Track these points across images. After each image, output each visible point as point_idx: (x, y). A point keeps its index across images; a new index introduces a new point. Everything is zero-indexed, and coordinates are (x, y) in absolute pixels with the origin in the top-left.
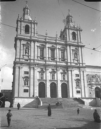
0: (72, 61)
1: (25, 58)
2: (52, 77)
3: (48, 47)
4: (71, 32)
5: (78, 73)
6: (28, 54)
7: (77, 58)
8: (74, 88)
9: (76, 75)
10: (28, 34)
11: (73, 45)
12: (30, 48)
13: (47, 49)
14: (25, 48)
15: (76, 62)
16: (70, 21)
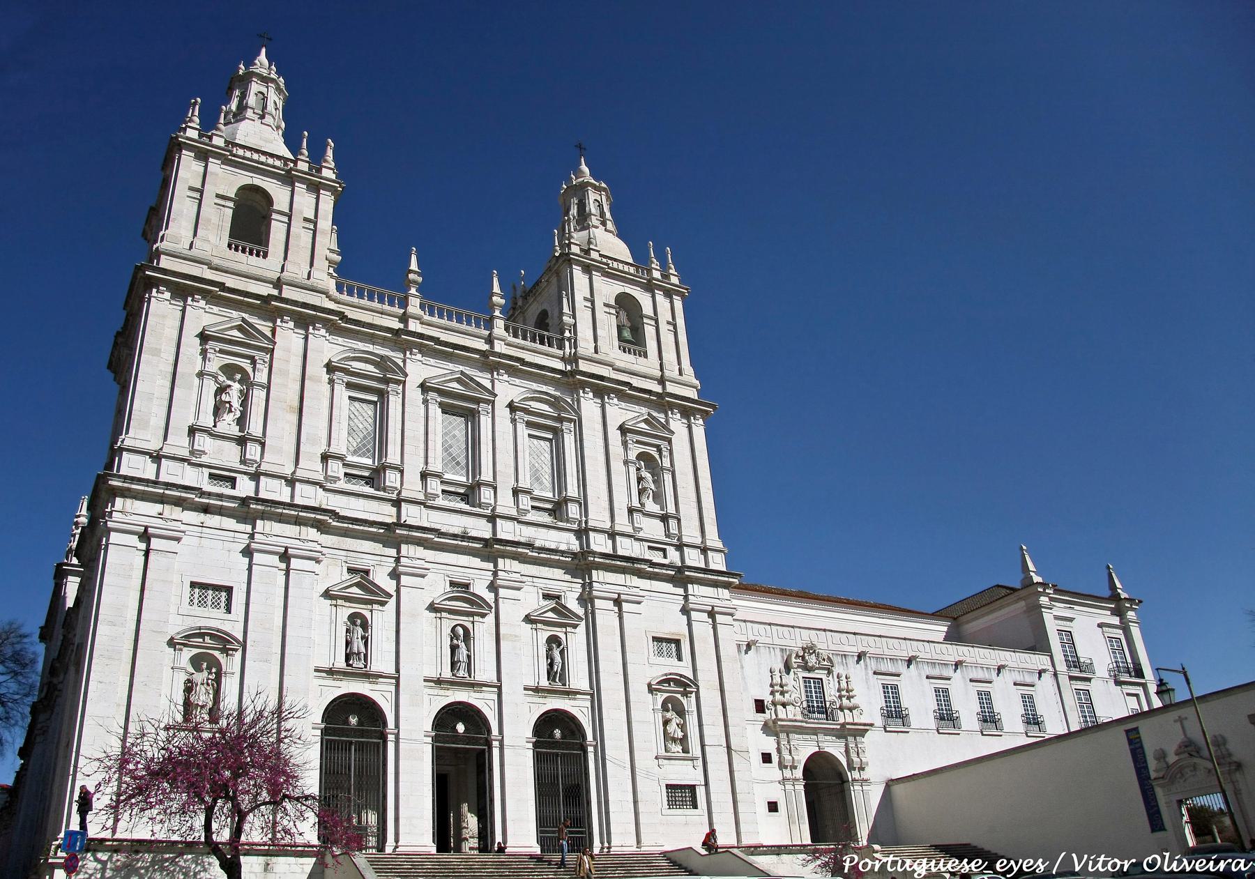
0: (622, 523)
1: (204, 459)
2: (454, 649)
3: (424, 387)
5: (675, 625)
6: (242, 421)
7: (658, 497)
8: (645, 760)
9: (655, 639)
10: (253, 260)
11: (626, 393)
12: (262, 377)
13: (414, 395)
14: (215, 363)
15: (654, 529)
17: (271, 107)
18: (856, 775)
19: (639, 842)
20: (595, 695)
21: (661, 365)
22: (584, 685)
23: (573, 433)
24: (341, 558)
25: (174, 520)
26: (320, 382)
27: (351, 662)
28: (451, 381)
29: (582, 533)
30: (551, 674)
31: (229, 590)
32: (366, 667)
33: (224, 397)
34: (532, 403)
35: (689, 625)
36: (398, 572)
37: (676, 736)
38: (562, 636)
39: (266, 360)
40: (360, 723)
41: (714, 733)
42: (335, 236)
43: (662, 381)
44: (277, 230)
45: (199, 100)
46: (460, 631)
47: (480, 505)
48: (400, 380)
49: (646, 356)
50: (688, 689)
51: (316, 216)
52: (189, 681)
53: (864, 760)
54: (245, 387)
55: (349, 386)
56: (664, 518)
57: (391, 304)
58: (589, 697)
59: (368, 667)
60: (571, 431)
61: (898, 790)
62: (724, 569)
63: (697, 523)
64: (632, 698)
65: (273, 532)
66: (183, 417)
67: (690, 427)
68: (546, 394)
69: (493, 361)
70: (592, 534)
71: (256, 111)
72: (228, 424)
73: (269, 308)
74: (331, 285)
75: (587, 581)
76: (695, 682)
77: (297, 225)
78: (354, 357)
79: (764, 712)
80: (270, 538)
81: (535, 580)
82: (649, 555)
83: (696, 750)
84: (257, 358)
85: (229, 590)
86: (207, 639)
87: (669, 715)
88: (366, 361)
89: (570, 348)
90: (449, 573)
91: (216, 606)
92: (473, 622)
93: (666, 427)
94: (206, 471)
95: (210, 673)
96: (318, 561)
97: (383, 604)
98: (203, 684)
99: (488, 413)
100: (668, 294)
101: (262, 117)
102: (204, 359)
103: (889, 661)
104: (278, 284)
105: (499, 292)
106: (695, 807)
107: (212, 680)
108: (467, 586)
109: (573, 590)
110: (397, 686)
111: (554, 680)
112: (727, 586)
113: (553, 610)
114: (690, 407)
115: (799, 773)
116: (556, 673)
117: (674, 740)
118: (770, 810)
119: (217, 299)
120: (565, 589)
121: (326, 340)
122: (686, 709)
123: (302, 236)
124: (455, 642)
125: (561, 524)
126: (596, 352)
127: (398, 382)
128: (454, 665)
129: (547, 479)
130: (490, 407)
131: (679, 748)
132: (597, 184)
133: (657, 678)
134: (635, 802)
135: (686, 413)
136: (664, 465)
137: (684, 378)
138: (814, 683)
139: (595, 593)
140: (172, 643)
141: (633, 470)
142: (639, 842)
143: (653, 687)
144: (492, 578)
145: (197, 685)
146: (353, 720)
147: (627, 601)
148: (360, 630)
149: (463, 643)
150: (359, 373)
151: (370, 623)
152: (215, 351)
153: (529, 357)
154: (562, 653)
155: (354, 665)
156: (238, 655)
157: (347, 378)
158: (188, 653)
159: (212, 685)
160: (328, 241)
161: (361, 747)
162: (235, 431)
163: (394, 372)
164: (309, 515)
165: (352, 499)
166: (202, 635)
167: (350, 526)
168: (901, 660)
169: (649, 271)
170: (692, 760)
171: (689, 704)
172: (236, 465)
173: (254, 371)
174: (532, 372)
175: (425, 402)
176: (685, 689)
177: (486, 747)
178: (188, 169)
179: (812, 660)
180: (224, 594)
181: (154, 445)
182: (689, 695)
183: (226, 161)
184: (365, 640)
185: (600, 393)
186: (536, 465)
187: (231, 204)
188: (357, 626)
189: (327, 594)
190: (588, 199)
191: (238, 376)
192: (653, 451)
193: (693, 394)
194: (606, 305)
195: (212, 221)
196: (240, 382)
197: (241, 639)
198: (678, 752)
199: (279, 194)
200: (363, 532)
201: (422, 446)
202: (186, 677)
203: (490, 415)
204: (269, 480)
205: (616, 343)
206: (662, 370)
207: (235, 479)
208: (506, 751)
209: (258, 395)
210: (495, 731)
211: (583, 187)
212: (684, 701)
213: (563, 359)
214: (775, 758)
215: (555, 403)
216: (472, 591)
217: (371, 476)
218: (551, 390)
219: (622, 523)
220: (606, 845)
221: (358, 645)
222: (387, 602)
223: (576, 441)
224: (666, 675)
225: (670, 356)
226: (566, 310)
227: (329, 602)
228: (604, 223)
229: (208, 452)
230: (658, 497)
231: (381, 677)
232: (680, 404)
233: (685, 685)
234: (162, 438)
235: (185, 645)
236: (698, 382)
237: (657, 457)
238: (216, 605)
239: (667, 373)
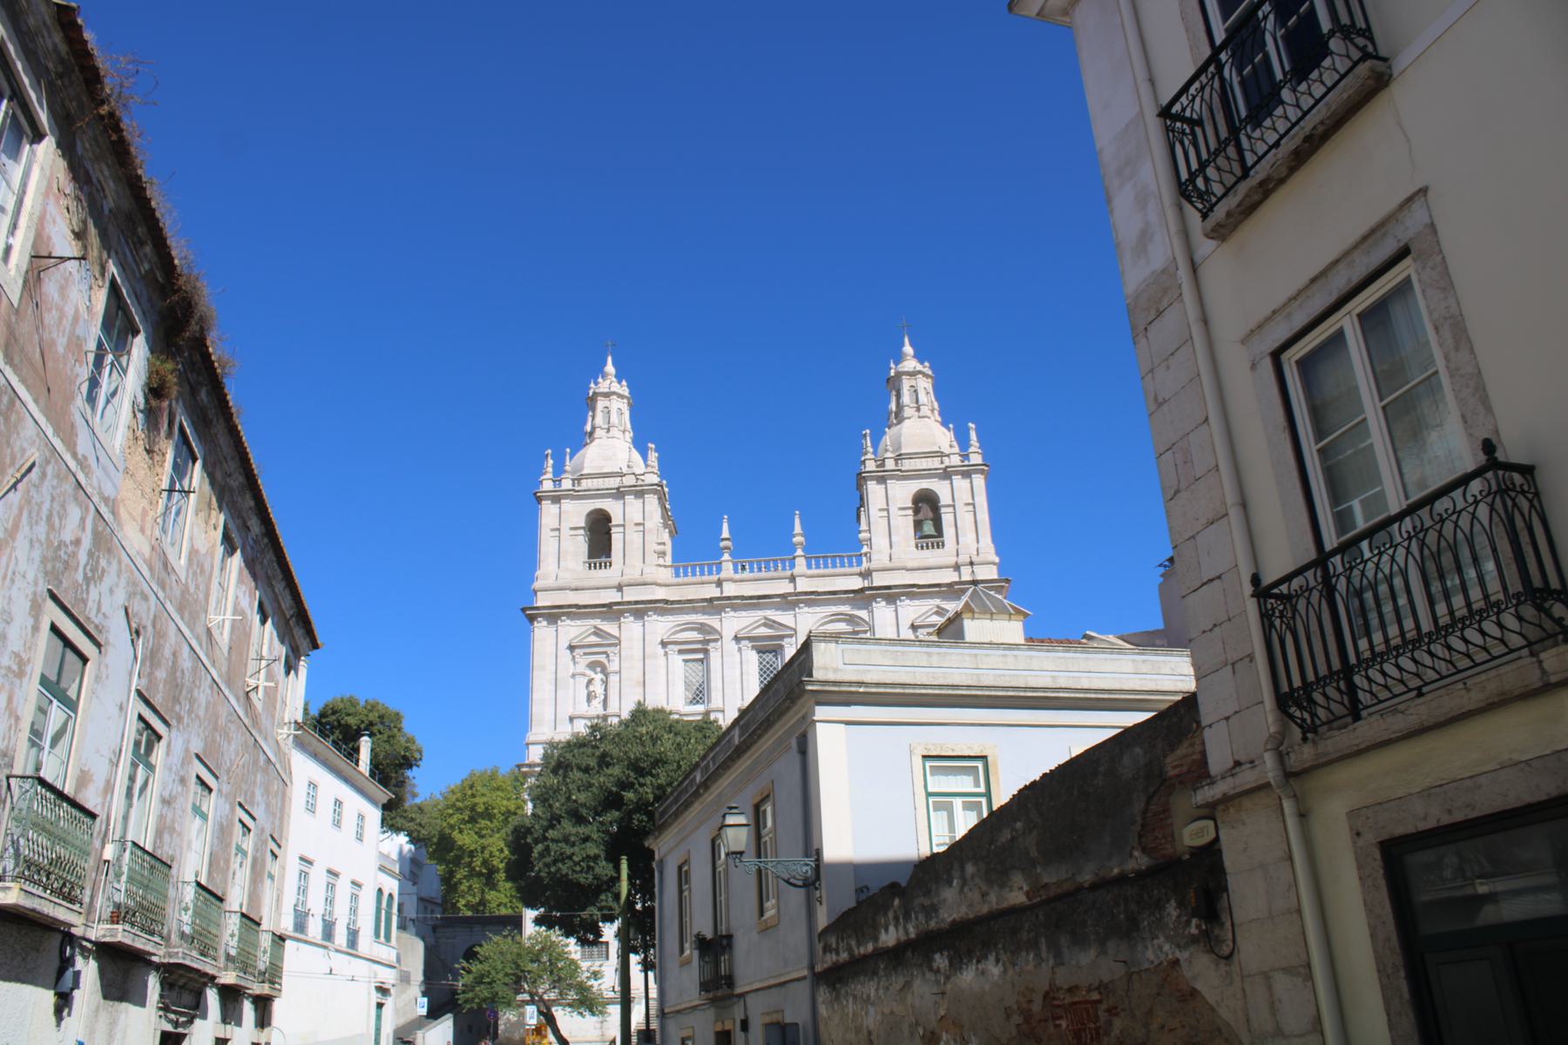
3: (737, 639)
4: (903, 492)
17: (614, 418)
33: (591, 689)
55: (681, 652)
73: (611, 611)
77: (630, 529)
101: (608, 431)
127: (716, 640)
178: (548, 511)
187: (582, 532)
201: (738, 686)
209: (613, 679)
215: (851, 619)
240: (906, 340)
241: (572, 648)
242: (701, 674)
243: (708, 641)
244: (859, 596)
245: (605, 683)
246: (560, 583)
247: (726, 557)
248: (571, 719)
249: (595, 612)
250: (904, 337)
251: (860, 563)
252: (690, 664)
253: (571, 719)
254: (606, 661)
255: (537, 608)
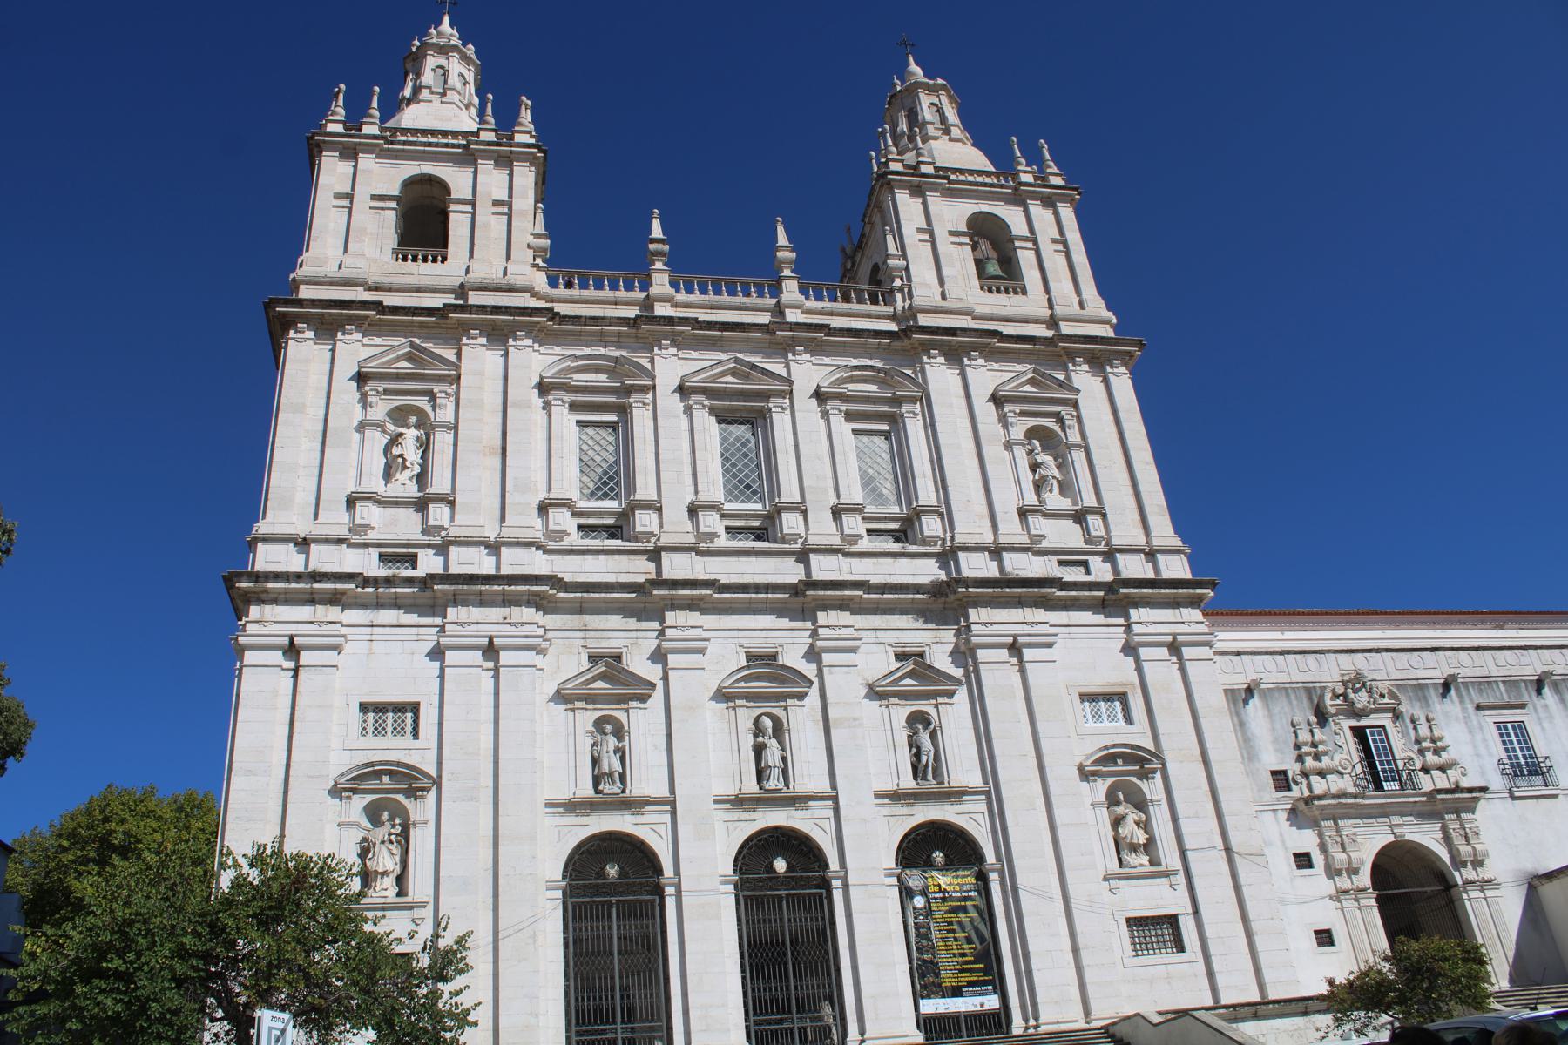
0: (1011, 531)
1: (372, 536)
2: (759, 750)
3: (683, 390)
4: (952, 213)
5: (1116, 672)
6: (422, 479)
8: (1085, 885)
10: (429, 268)
14: (380, 408)
15: (1066, 535)
16: (931, 130)
17: (454, 80)
18: (1469, 873)
19: (1087, 1012)
20: (992, 794)
21: (1050, 300)
22: (974, 779)
23: (920, 417)
24: (578, 641)
25: (331, 622)
26: (530, 407)
27: (601, 788)
28: (723, 374)
29: (948, 556)
30: (917, 770)
31: (415, 708)
32: (623, 791)
33: (396, 451)
34: (851, 386)
35: (1139, 669)
36: (663, 652)
37: (1135, 841)
38: (931, 710)
39: (449, 391)
40: (622, 874)
41: (1200, 829)
42: (540, 217)
43: (1053, 322)
44: (458, 225)
45: (343, 86)
46: (768, 723)
47: (783, 538)
48: (645, 386)
49: (1024, 292)
50: (1146, 766)
51: (510, 196)
52: (365, 839)
53: (1478, 847)
54: (422, 432)
55: (574, 407)
56: (1079, 517)
57: (629, 288)
58: (983, 797)
59: (628, 791)
60: (915, 414)
61: (1548, 891)
62: (1188, 576)
63: (1136, 516)
64: (1053, 790)
65: (470, 620)
66: (341, 483)
67: (1106, 381)
68: (871, 368)
69: (783, 337)
70: (962, 556)
71: (434, 90)
72: (404, 486)
74: (540, 280)
75: (963, 624)
76: (1158, 755)
77: (485, 212)
78: (578, 367)
79: (1289, 789)
80: (467, 628)
81: (880, 634)
82: (1055, 571)
83: (1171, 859)
84: (436, 391)
85: (415, 708)
86: (386, 779)
87: (1120, 810)
88: (597, 370)
89: (904, 301)
90: (743, 642)
91: (399, 732)
92: (786, 708)
93: (1066, 385)
94: (375, 552)
95: (393, 826)
96: (541, 651)
97: (643, 699)
98: (383, 842)
99: (783, 409)
100: (1049, 202)
101: (444, 94)
102: (364, 408)
103: (1501, 685)
104: (462, 291)
105: (787, 244)
106: (1182, 949)
107: (397, 835)
108: (774, 656)
109: (943, 640)
110: (674, 813)
111: (924, 778)
112: (1194, 602)
113: (910, 674)
114: (1101, 350)
115: (1365, 879)
116: (926, 766)
117: (1134, 848)
118: (1320, 944)
119: (377, 325)
120: (928, 641)
121: (534, 351)
122: (1149, 797)
123: (492, 225)
124: (761, 739)
125: (913, 548)
126: (944, 298)
127: (643, 390)
128: (761, 775)
129: (887, 488)
130: (787, 401)
131: (1145, 859)
132: (931, 82)
133: (1092, 754)
134: (1076, 951)
135: (1098, 363)
136: (1070, 439)
137: (1087, 313)
138: (1372, 734)
139: (974, 640)
140: (336, 792)
141: (1021, 454)
142: (1087, 1012)
143: (1087, 768)
144: (810, 640)
145: (374, 844)
146: (612, 871)
147: (1030, 645)
148: (612, 742)
149: (774, 742)
150: (586, 387)
151: (626, 728)
152: (378, 392)
153: (836, 322)
154: (933, 735)
155: (605, 791)
156: (432, 795)
157: (568, 398)
158: (360, 802)
159: (399, 842)
160: (529, 225)
161: (627, 911)
162: (412, 491)
163: (634, 376)
164: (519, 588)
165: (589, 559)
166: (378, 774)
167: (585, 595)
168: (1525, 681)
169: (1015, 176)
170: (1167, 876)
171: (1153, 789)
172: (415, 534)
173: (434, 409)
174: (845, 342)
175: (688, 410)
176: (1142, 767)
177: (824, 891)
178: (332, 172)
179: (1361, 700)
180: (409, 715)
181: (302, 528)
182: (1150, 775)
183: (383, 154)
184: (622, 753)
185: (955, 356)
186: (870, 471)
188: (606, 734)
189: (560, 697)
190: (920, 104)
191: (413, 420)
192: (1051, 424)
193: (1107, 332)
194: (952, 233)
195: (369, 231)
196: (417, 427)
197: (434, 774)
198: (1142, 865)
199: (457, 179)
200: (605, 601)
201: (688, 470)
202: (363, 835)
203: (788, 412)
204: (463, 549)
205: (975, 282)
206: (1051, 307)
207: (415, 556)
208: (852, 891)
209: (442, 440)
210: (834, 864)
211: (912, 90)
212: (1144, 785)
213: (893, 317)
214: (1318, 859)
215: (883, 378)
216: (781, 662)
217: (619, 524)
218: (878, 363)
219: (1011, 531)
220: (1032, 1022)
221: (611, 762)
222: (650, 696)
223: (926, 427)
224: (1106, 748)
225: (1062, 285)
226: (892, 249)
227: (563, 707)
228: (947, 131)
229: (377, 526)
230: (1066, 488)
231: (648, 803)
232: (1085, 349)
233: (1142, 761)
234: (312, 517)
235: (354, 791)
236: (1110, 314)
237: (1057, 428)
238: (398, 730)
239: (1058, 310)
240: (911, 59)
241: (361, 378)
242: (611, 449)
243: (628, 391)
244: (897, 344)
245: (425, 446)
246: (345, 273)
247: (659, 265)
248: (351, 502)
249: (411, 324)
250: (907, 54)
251: (889, 301)
252: (590, 431)
253: (351, 502)
254: (428, 408)
255: (301, 303)
